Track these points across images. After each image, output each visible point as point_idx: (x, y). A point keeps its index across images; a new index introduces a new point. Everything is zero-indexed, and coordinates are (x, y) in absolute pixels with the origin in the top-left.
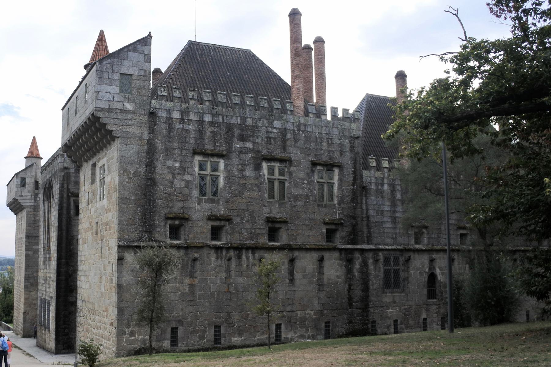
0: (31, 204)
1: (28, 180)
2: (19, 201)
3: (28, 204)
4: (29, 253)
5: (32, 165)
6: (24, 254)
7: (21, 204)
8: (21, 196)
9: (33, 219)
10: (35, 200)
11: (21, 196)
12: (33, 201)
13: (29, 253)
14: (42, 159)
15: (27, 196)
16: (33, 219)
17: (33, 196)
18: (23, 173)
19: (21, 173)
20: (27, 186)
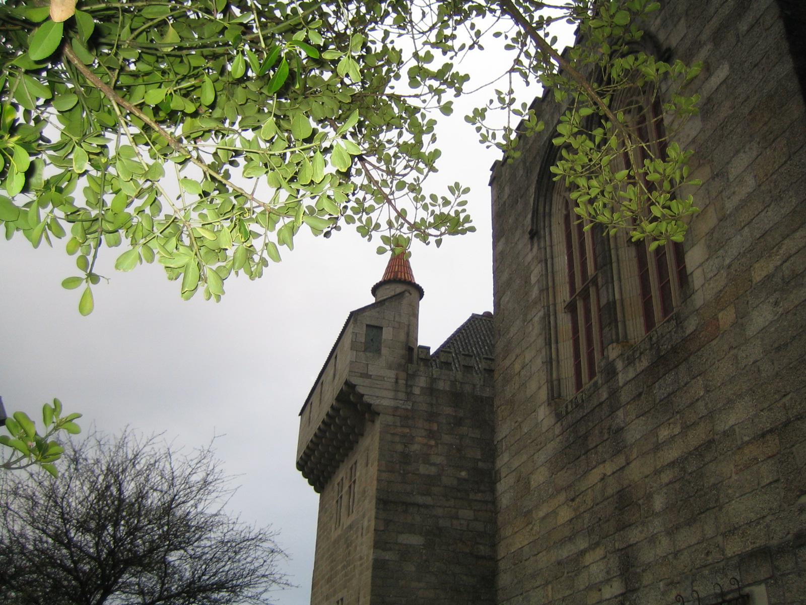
0: (392, 403)
1: (387, 334)
2: (360, 390)
3: (385, 403)
4: (388, 556)
5: (400, 295)
6: (370, 563)
7: (366, 399)
8: (366, 376)
9: (400, 448)
10: (409, 394)
11: (366, 376)
12: (402, 395)
13: (388, 556)
14: (420, 292)
15: (382, 378)
16: (400, 448)
17: (402, 382)
18: (374, 313)
19: (367, 313)
20: (384, 351)
